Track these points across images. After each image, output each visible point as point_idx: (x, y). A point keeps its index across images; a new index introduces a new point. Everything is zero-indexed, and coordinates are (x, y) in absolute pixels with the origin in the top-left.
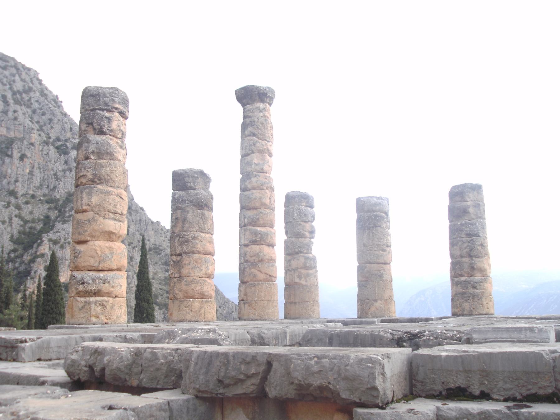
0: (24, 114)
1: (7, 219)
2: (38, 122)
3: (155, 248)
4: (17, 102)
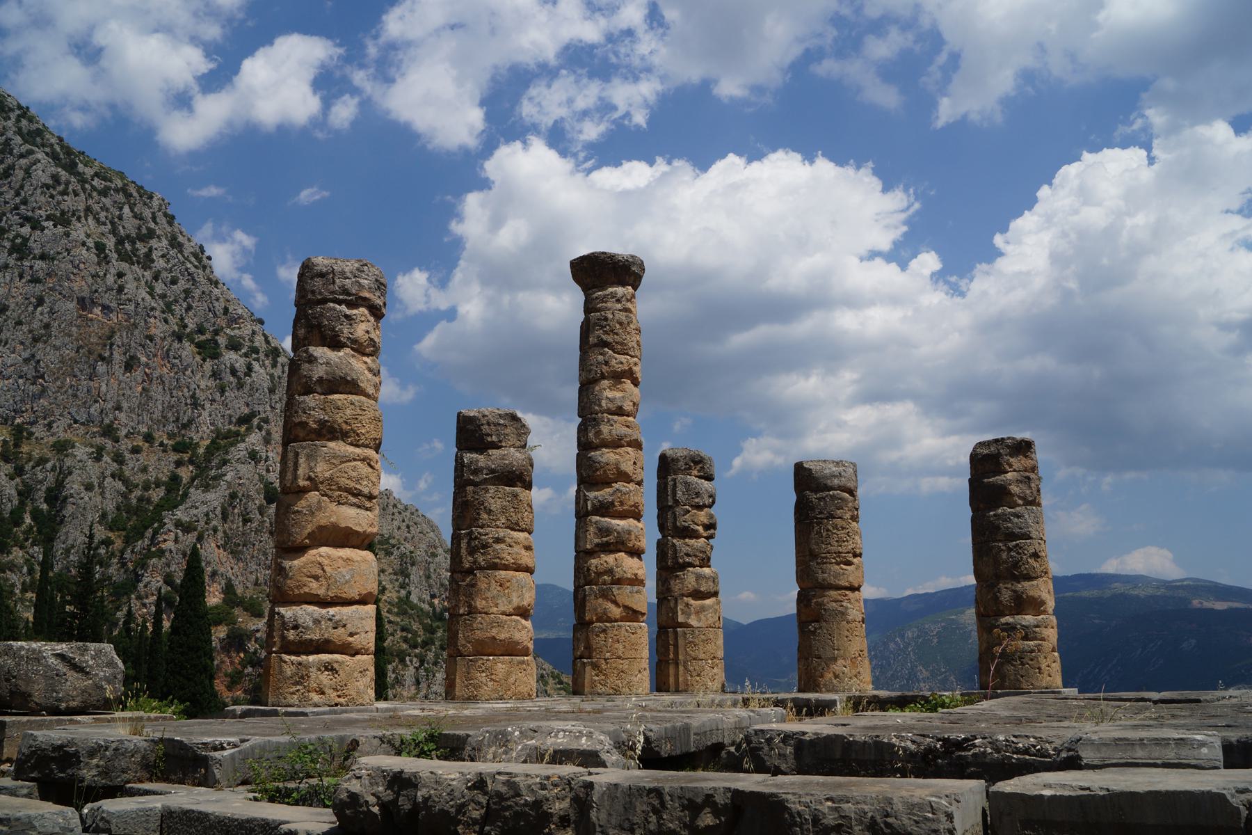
0: (137, 279)
2: (163, 296)
4: (123, 257)
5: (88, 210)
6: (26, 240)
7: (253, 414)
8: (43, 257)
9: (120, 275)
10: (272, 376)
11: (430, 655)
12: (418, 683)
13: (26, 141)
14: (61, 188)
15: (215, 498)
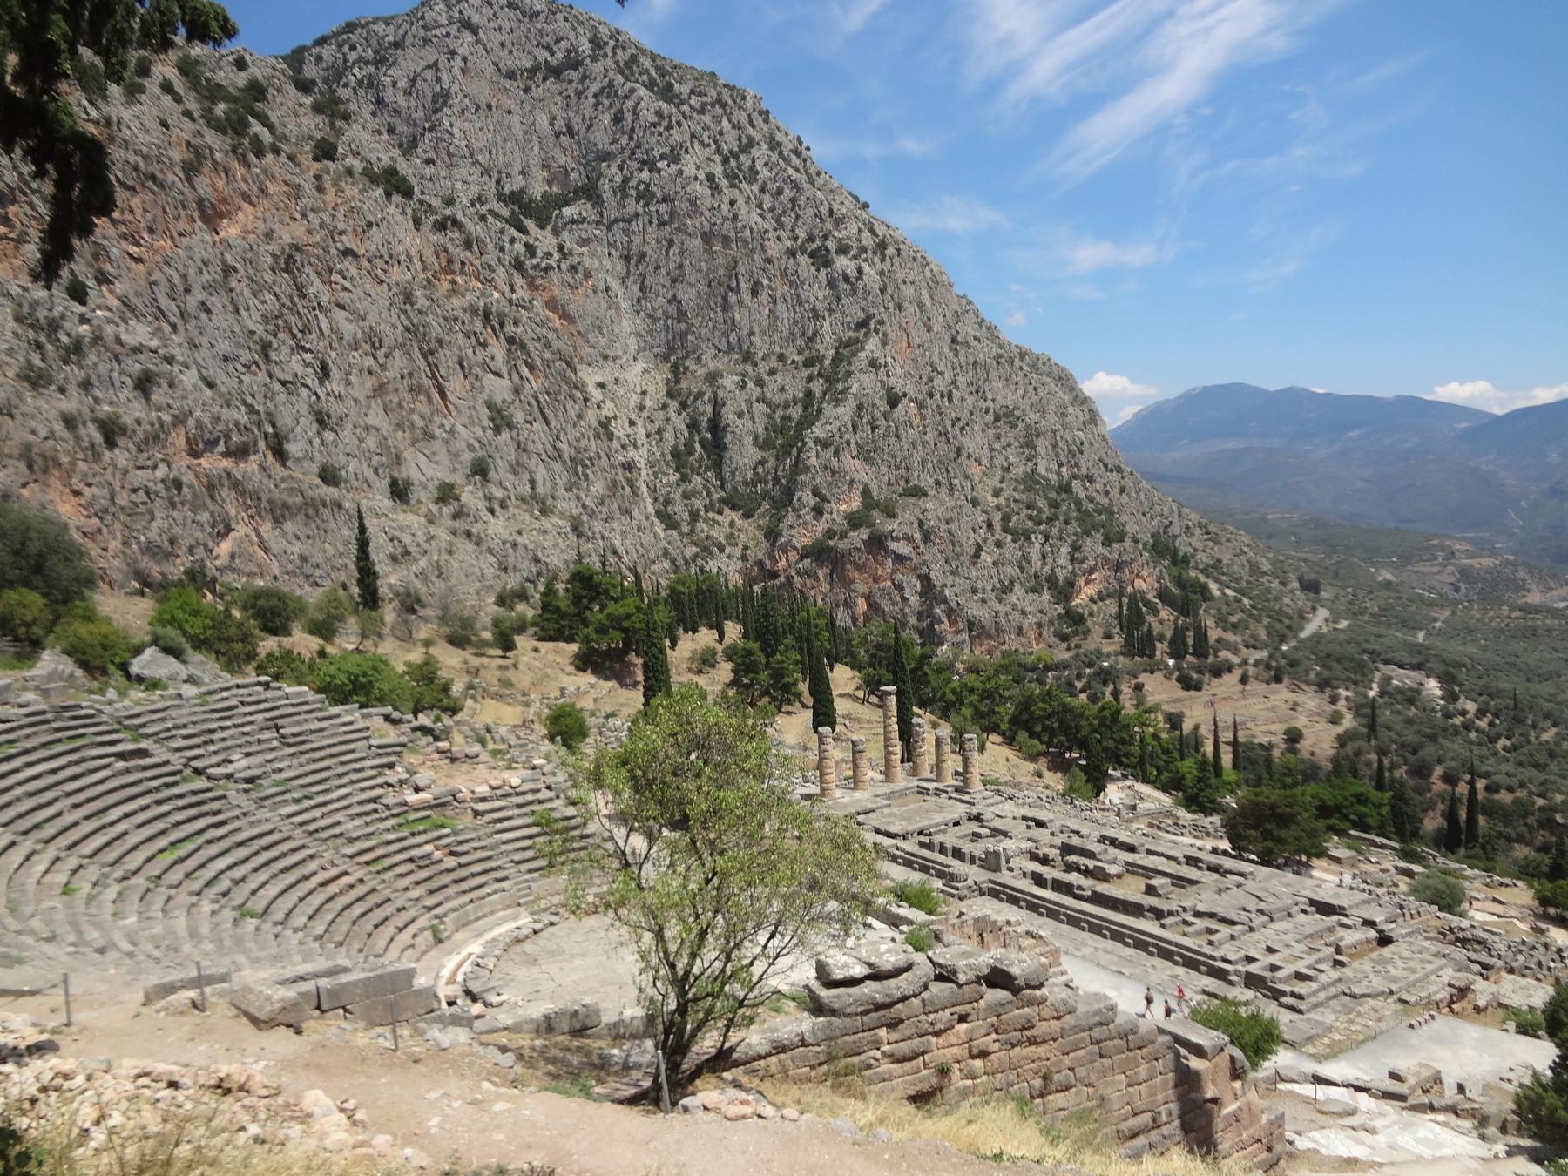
1: (744, 408)
2: (772, 209)
3: (1005, 415)
5: (693, 135)
6: (648, 185)
7: (869, 318)
8: (664, 200)
9: (732, 203)
10: (882, 273)
11: (1055, 531)
12: (1044, 557)
13: (627, 79)
14: (665, 123)
15: (845, 412)
